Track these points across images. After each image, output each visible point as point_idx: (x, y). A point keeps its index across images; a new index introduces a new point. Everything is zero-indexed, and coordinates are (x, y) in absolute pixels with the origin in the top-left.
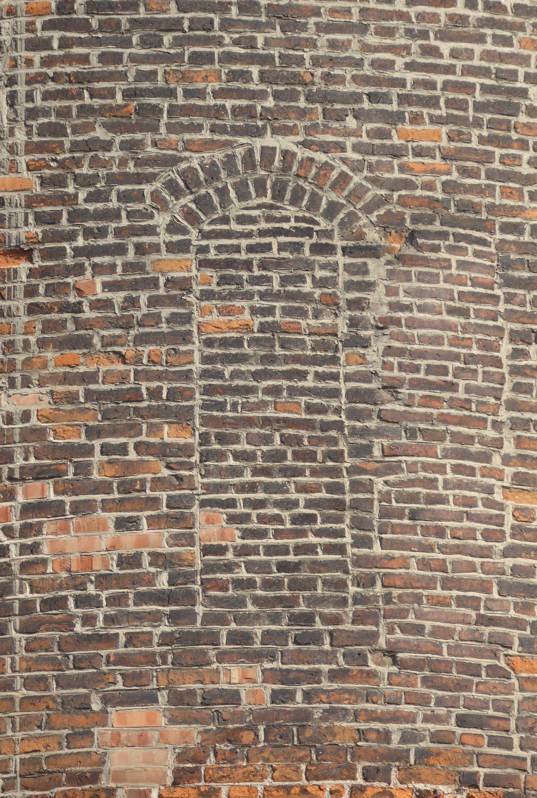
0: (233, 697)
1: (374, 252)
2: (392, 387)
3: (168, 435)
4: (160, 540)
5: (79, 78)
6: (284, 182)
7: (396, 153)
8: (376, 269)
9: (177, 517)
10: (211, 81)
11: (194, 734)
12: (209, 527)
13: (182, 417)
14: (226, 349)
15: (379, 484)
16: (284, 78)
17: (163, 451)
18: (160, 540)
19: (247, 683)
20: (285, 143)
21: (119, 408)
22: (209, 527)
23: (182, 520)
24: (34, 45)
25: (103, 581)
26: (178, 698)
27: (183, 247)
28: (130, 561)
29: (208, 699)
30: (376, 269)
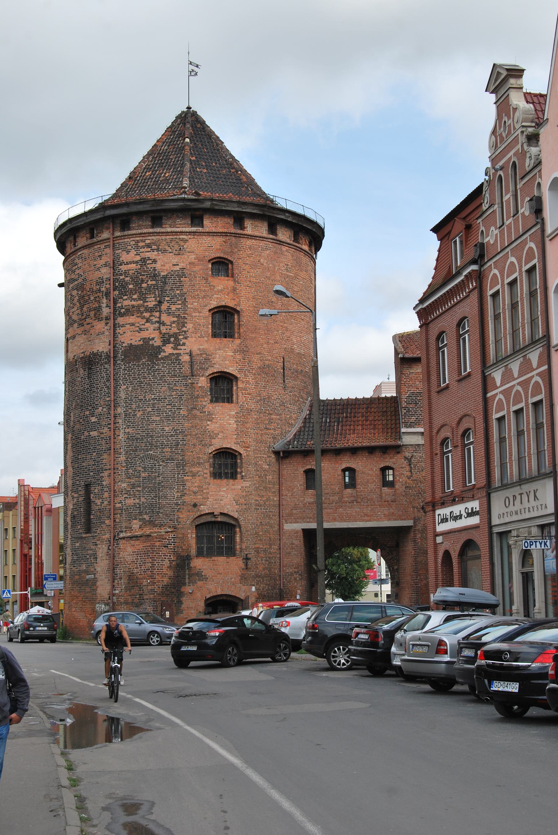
0: (145, 519)
1: (161, 465)
2: (162, 482)
3: (139, 489)
4: (137, 501)
5: (130, 445)
6: (151, 457)
7: (164, 452)
8: (161, 467)
9: (139, 499)
10: (143, 445)
11: (141, 523)
12: (143, 500)
13: (140, 486)
14: (144, 478)
15: (161, 493)
16: (151, 444)
17: (138, 491)
18: (137, 501)
19: (146, 517)
20: (151, 452)
21: (133, 486)
22: (143, 500)
23: (140, 499)
24: (125, 441)
25: (132, 506)
26: (140, 519)
27: (140, 466)
28: (134, 504)
29: (143, 519)
30: (161, 467)
